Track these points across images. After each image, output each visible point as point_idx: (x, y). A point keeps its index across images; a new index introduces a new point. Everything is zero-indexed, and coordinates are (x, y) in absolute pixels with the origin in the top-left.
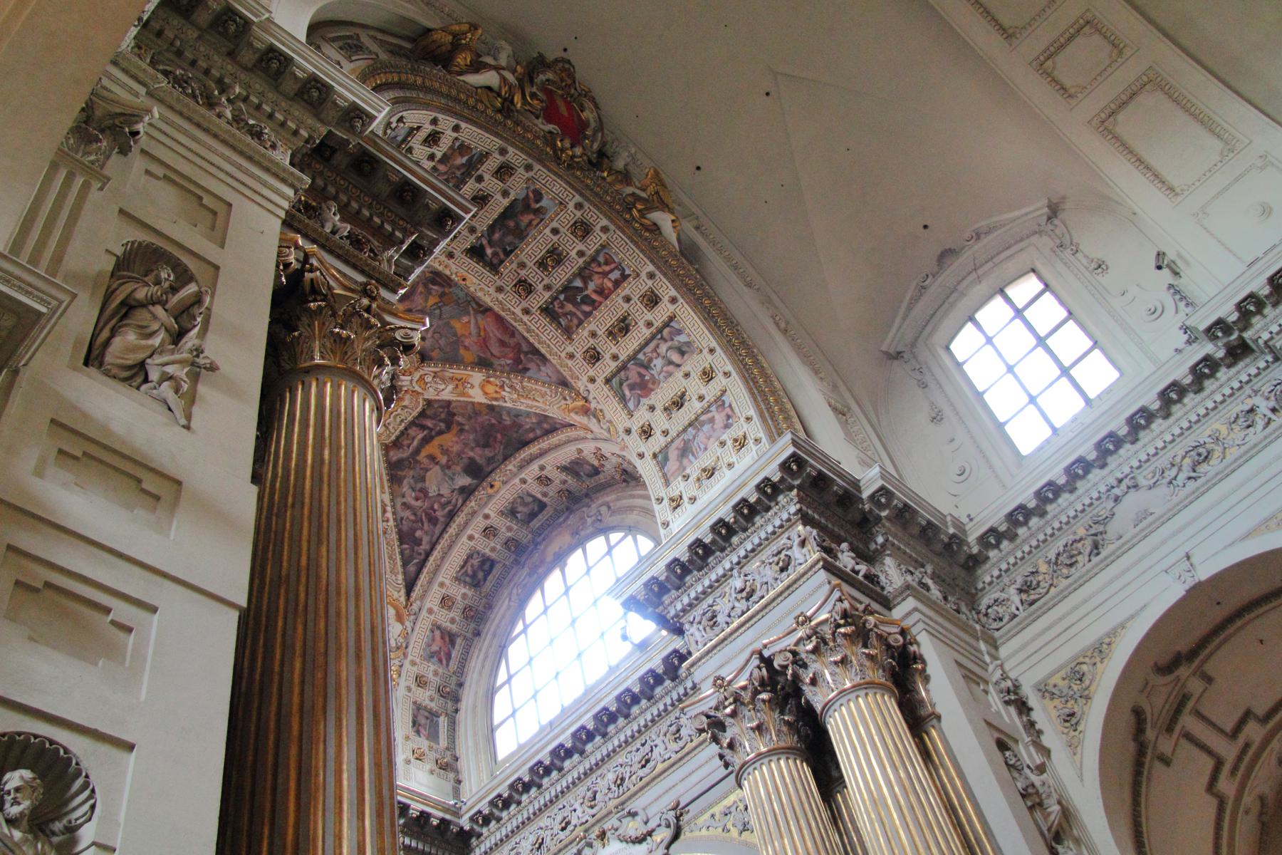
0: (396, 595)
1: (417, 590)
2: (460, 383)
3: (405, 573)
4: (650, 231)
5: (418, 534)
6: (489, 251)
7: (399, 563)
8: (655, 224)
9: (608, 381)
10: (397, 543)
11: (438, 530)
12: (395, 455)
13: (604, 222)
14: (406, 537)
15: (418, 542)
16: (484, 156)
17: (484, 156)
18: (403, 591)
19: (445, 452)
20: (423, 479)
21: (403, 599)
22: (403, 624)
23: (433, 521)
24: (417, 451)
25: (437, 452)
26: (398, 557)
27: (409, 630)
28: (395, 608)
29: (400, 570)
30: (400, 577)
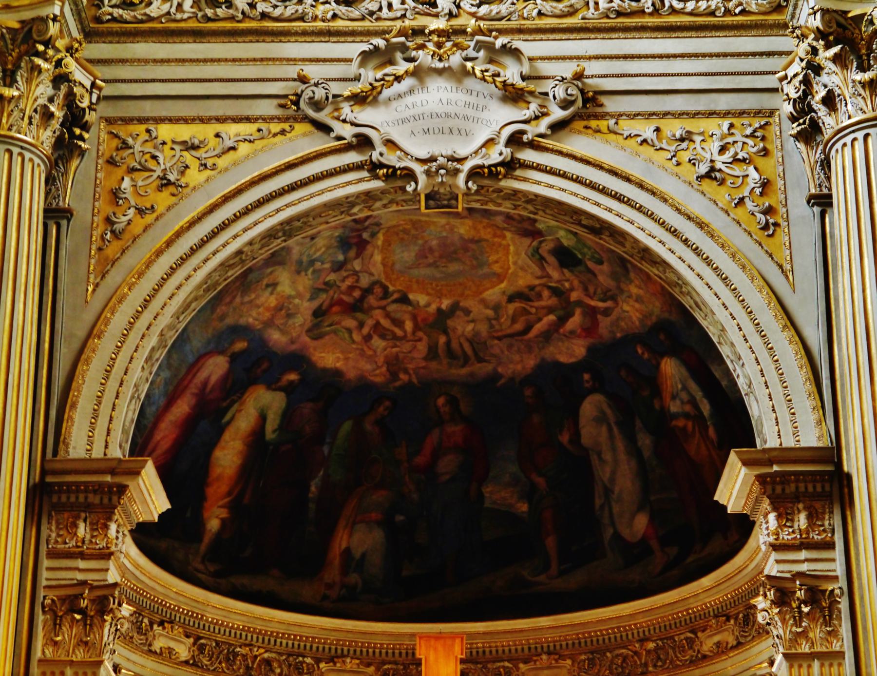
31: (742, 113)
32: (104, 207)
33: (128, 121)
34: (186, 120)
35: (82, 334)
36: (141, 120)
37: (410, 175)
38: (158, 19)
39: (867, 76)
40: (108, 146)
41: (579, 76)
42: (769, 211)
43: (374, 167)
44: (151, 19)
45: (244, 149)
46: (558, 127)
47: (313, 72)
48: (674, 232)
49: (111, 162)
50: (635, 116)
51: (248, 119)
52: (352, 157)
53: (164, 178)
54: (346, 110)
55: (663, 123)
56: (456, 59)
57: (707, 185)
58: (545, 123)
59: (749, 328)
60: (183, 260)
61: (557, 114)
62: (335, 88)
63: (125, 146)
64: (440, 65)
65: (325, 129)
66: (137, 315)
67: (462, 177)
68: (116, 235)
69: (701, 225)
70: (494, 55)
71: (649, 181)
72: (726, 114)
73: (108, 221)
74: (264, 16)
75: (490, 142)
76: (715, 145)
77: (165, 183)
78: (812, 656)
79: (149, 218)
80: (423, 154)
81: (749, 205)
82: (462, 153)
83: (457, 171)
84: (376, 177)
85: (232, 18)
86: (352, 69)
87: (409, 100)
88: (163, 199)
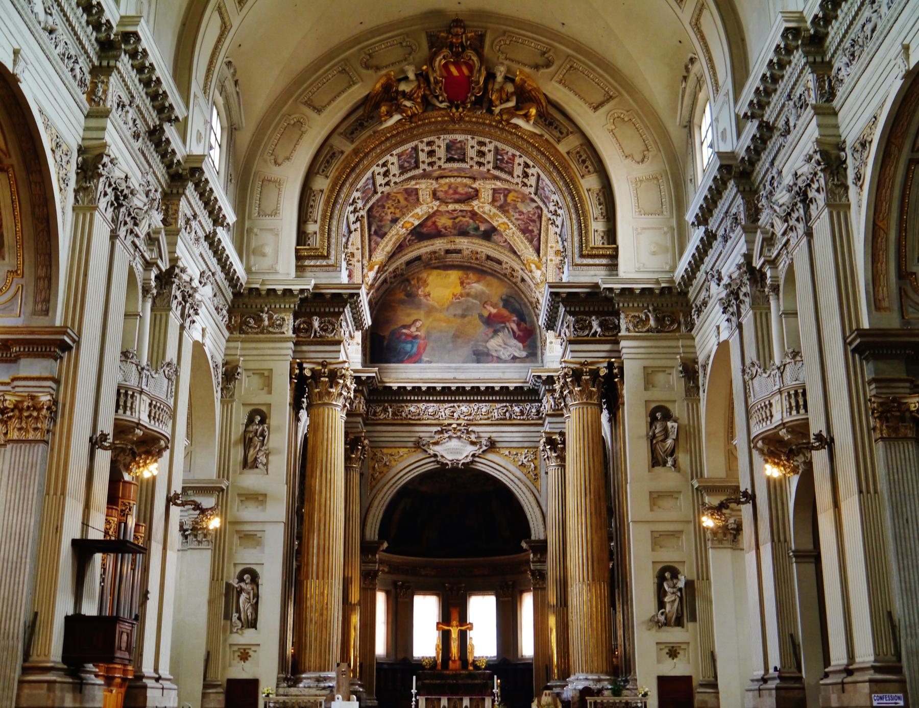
0: (532, 258)
1: (542, 252)
2: (495, 185)
3: (533, 246)
4: (515, 129)
5: (530, 228)
6: (456, 157)
7: (528, 244)
8: (515, 124)
9: (536, 194)
10: (522, 236)
11: (538, 225)
12: (498, 204)
13: (487, 140)
14: (524, 231)
15: (532, 231)
16: (417, 146)
17: (417, 146)
18: (535, 255)
19: (517, 198)
20: (517, 208)
21: (536, 259)
22: (540, 270)
23: (534, 221)
24: (505, 200)
25: (514, 199)
26: (526, 241)
27: (545, 271)
28: (534, 264)
29: (530, 246)
30: (531, 249)
31: (530, 448)
32: (371, 471)
33: (376, 447)
34: (391, 448)
35: (367, 506)
36: (380, 447)
37: (447, 464)
38: (383, 420)
39: (556, 455)
40: (371, 455)
41: (490, 438)
42: (536, 475)
43: (438, 462)
44: (380, 419)
45: (405, 456)
46: (483, 452)
47: (422, 435)
48: (512, 481)
49: (372, 459)
50: (503, 448)
51: (407, 448)
52: (432, 459)
53: (385, 464)
54: (431, 447)
55: (511, 450)
56: (459, 434)
57: (521, 467)
58: (481, 450)
59: (529, 506)
60: (391, 486)
61: (484, 448)
62: (428, 439)
63: (375, 454)
64: (455, 436)
65: (426, 452)
66: (380, 501)
67: (460, 465)
68: (374, 479)
69: (519, 479)
70: (468, 432)
71: (506, 467)
72: (526, 448)
73: (372, 475)
74: (410, 419)
75: (467, 456)
76: (523, 457)
77: (385, 465)
78: (539, 588)
79: (382, 475)
80: (450, 458)
81: (531, 473)
82: (460, 458)
83: (458, 464)
84: (438, 464)
85: (402, 419)
86: (433, 434)
87: (447, 444)
88: (385, 470)
